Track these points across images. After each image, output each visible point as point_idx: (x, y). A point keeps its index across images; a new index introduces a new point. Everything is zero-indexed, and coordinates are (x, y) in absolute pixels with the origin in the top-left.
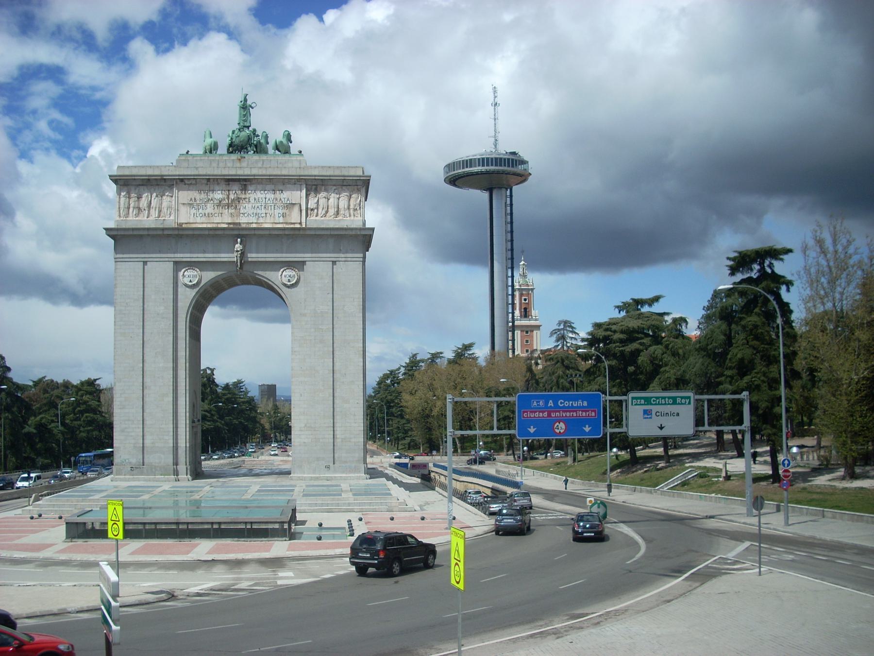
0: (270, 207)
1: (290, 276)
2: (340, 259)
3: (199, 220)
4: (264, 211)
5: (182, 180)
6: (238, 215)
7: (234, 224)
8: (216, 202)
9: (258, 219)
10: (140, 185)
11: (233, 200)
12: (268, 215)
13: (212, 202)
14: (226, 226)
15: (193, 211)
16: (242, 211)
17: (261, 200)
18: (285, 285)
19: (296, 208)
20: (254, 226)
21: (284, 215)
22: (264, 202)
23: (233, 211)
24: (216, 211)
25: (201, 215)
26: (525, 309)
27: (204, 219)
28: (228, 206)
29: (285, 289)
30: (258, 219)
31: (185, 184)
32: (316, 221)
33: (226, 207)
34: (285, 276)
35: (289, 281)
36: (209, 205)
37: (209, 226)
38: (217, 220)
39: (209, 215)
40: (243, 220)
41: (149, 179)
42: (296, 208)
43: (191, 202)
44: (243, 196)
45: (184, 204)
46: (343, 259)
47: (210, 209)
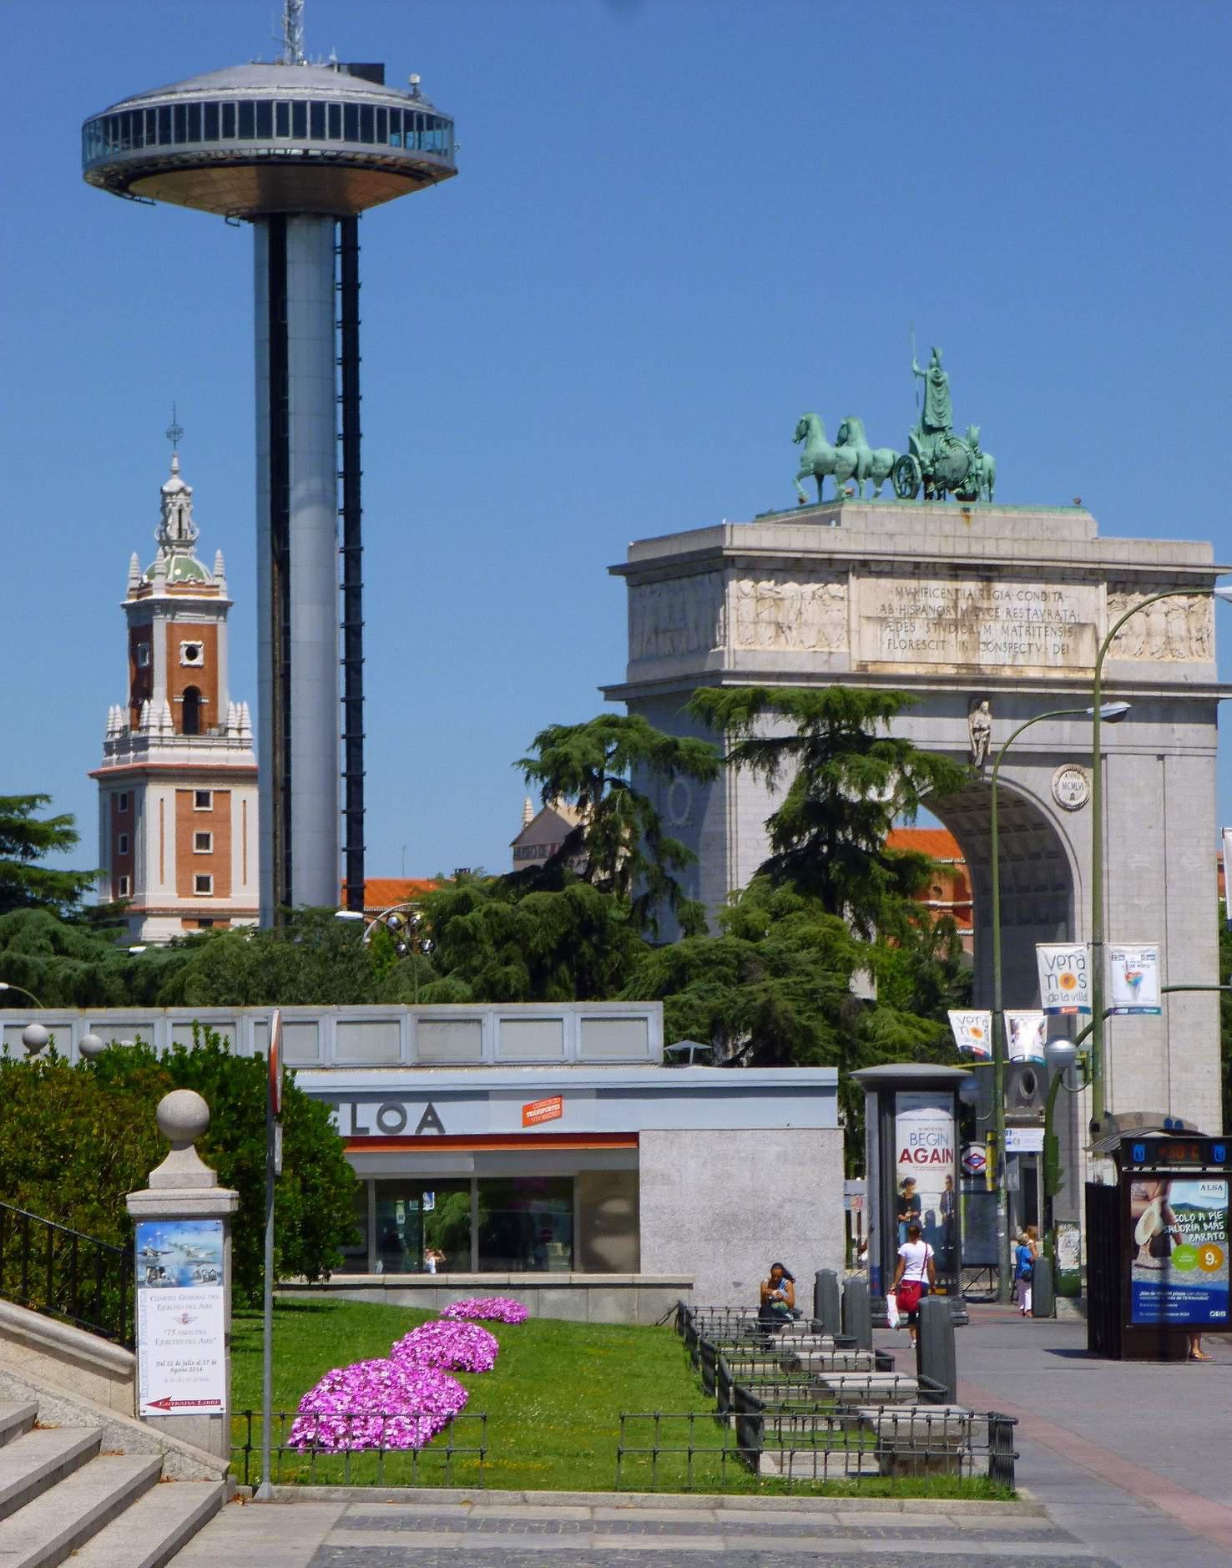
0: (1037, 630)
1: (1074, 786)
2: (1172, 751)
3: (899, 655)
4: (1025, 639)
5: (864, 563)
6: (976, 649)
7: (967, 666)
8: (931, 616)
9: (1014, 657)
10: (776, 570)
11: (964, 613)
12: (1034, 648)
13: (924, 615)
14: (950, 671)
15: (887, 634)
16: (983, 638)
17: (1019, 614)
18: (1065, 807)
19: (1088, 635)
20: (1007, 673)
21: (1064, 649)
22: (1025, 618)
23: (966, 637)
24: (934, 636)
25: (903, 645)
26: (192, 695)
27: (909, 655)
28: (956, 624)
29: (1062, 815)
30: (1014, 657)
31: (870, 572)
32: (1124, 663)
33: (953, 628)
34: (1064, 786)
35: (1073, 797)
36: (918, 622)
37: (921, 670)
38: (935, 656)
39: (922, 645)
40: (986, 659)
41: (830, 560)
42: (1088, 635)
43: (882, 615)
44: (985, 605)
45: (868, 618)
46: (1178, 751)
47: (920, 632)
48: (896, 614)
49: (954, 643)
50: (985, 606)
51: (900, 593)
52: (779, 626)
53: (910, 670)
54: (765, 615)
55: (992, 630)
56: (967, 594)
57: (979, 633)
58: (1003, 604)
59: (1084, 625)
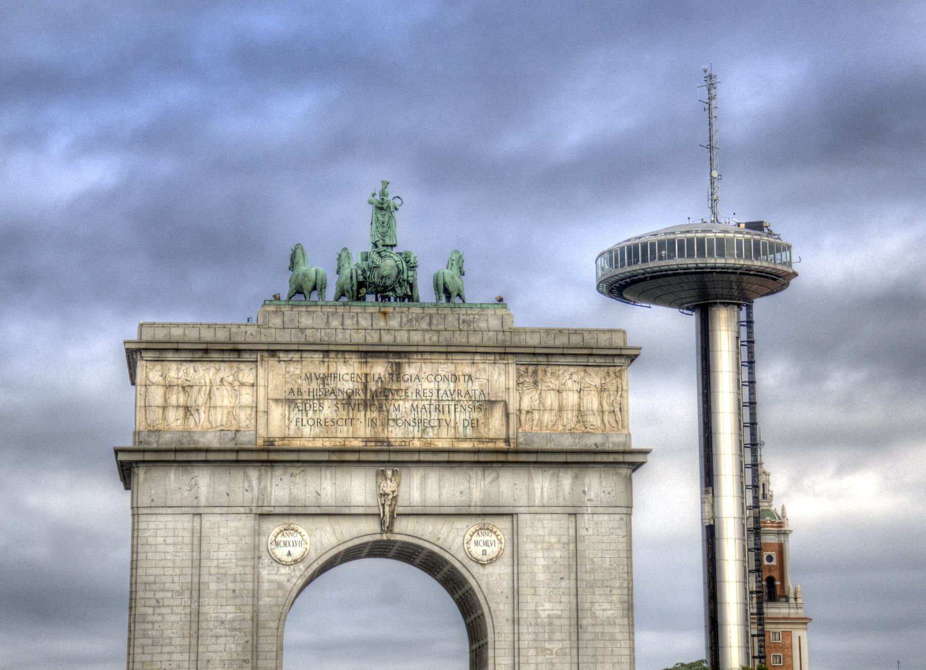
0: (446, 408)
4: (435, 415)
6: (385, 424)
7: (377, 441)
9: (424, 431)
12: (443, 423)
14: (357, 444)
18: (477, 561)
20: (417, 444)
22: (435, 397)
23: (375, 414)
28: (366, 405)
30: (424, 431)
33: (362, 408)
34: (477, 543)
35: (484, 553)
36: (326, 404)
37: (328, 444)
38: (343, 431)
42: (498, 413)
43: (291, 397)
47: (328, 410)
48: (306, 396)
49: (363, 421)
50: (394, 387)
51: (309, 378)
52: (187, 409)
53: (318, 444)
54: (173, 400)
55: (402, 407)
56: (376, 377)
57: (388, 411)
58: (413, 386)
59: (492, 403)
